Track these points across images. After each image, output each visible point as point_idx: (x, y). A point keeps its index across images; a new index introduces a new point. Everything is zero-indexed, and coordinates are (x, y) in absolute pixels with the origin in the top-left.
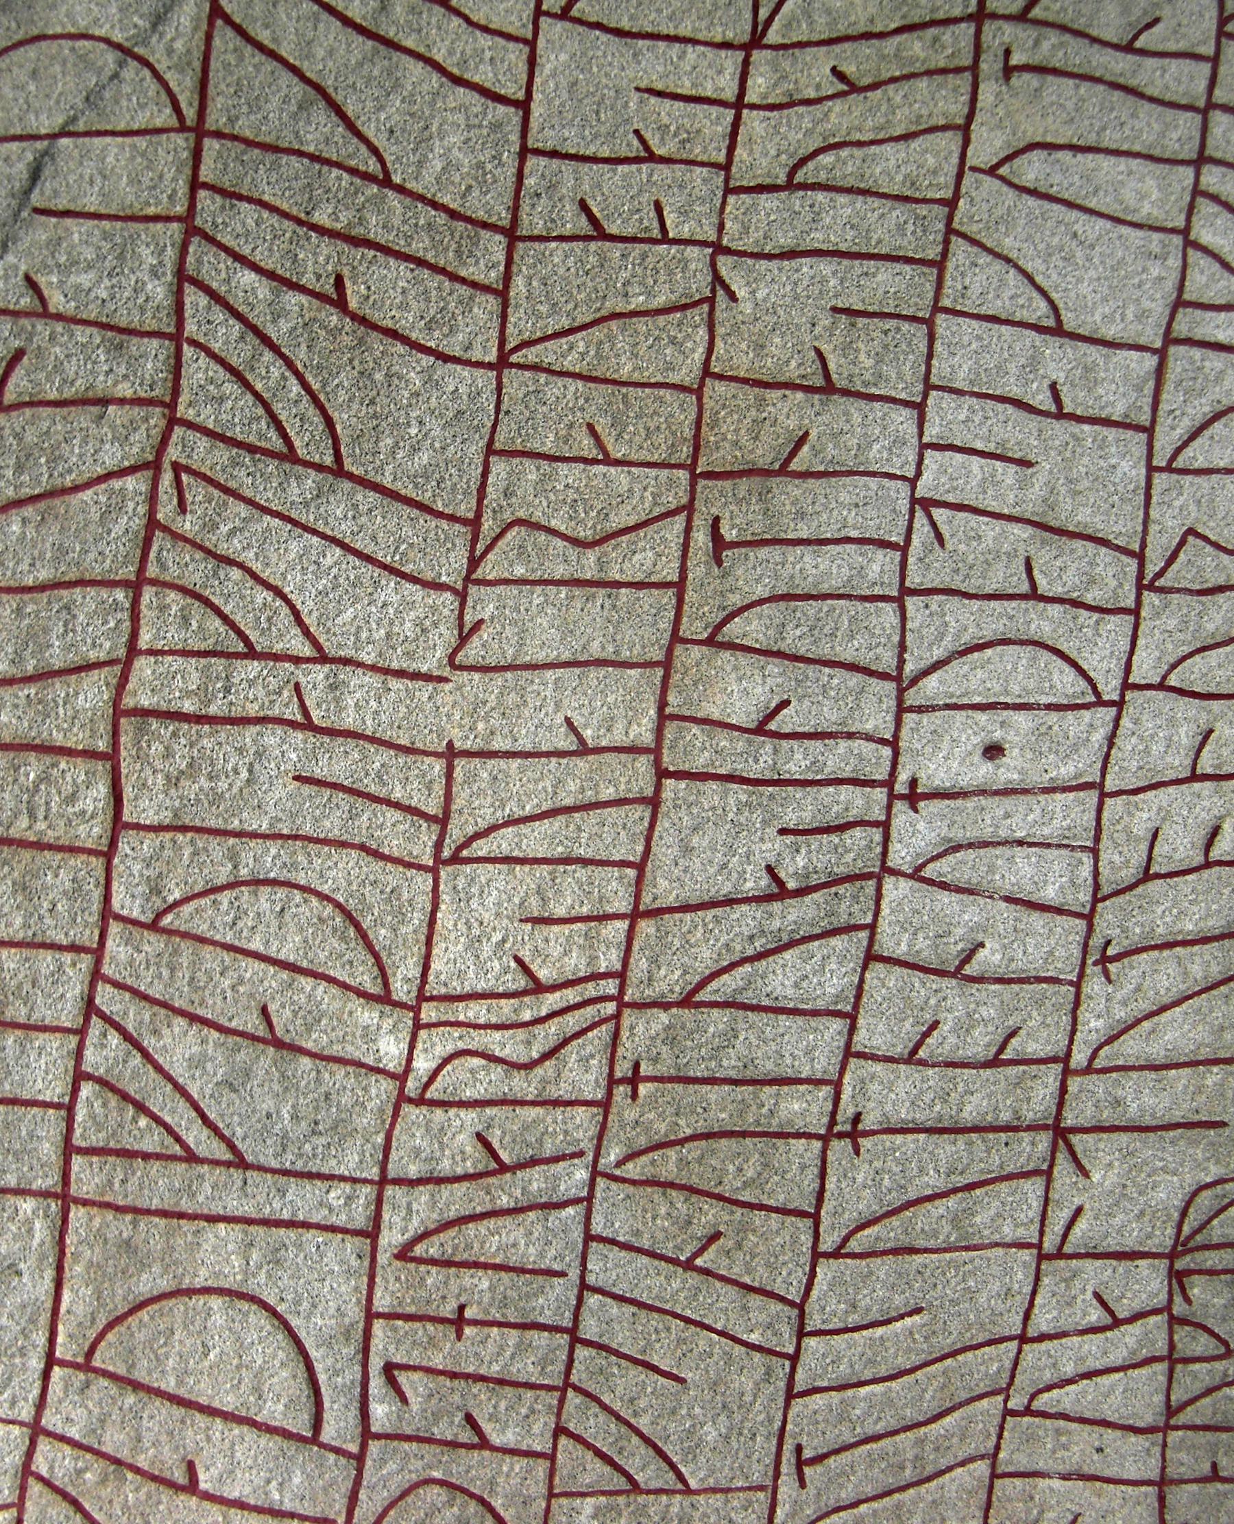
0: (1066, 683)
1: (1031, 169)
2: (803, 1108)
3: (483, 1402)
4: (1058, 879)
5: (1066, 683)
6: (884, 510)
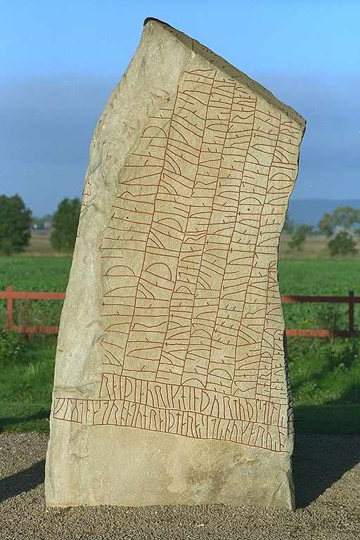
0: (257, 203)
1: (256, 147)
2: (226, 247)
3: (189, 277)
4: (256, 224)
5: (258, 203)
6: (238, 183)
